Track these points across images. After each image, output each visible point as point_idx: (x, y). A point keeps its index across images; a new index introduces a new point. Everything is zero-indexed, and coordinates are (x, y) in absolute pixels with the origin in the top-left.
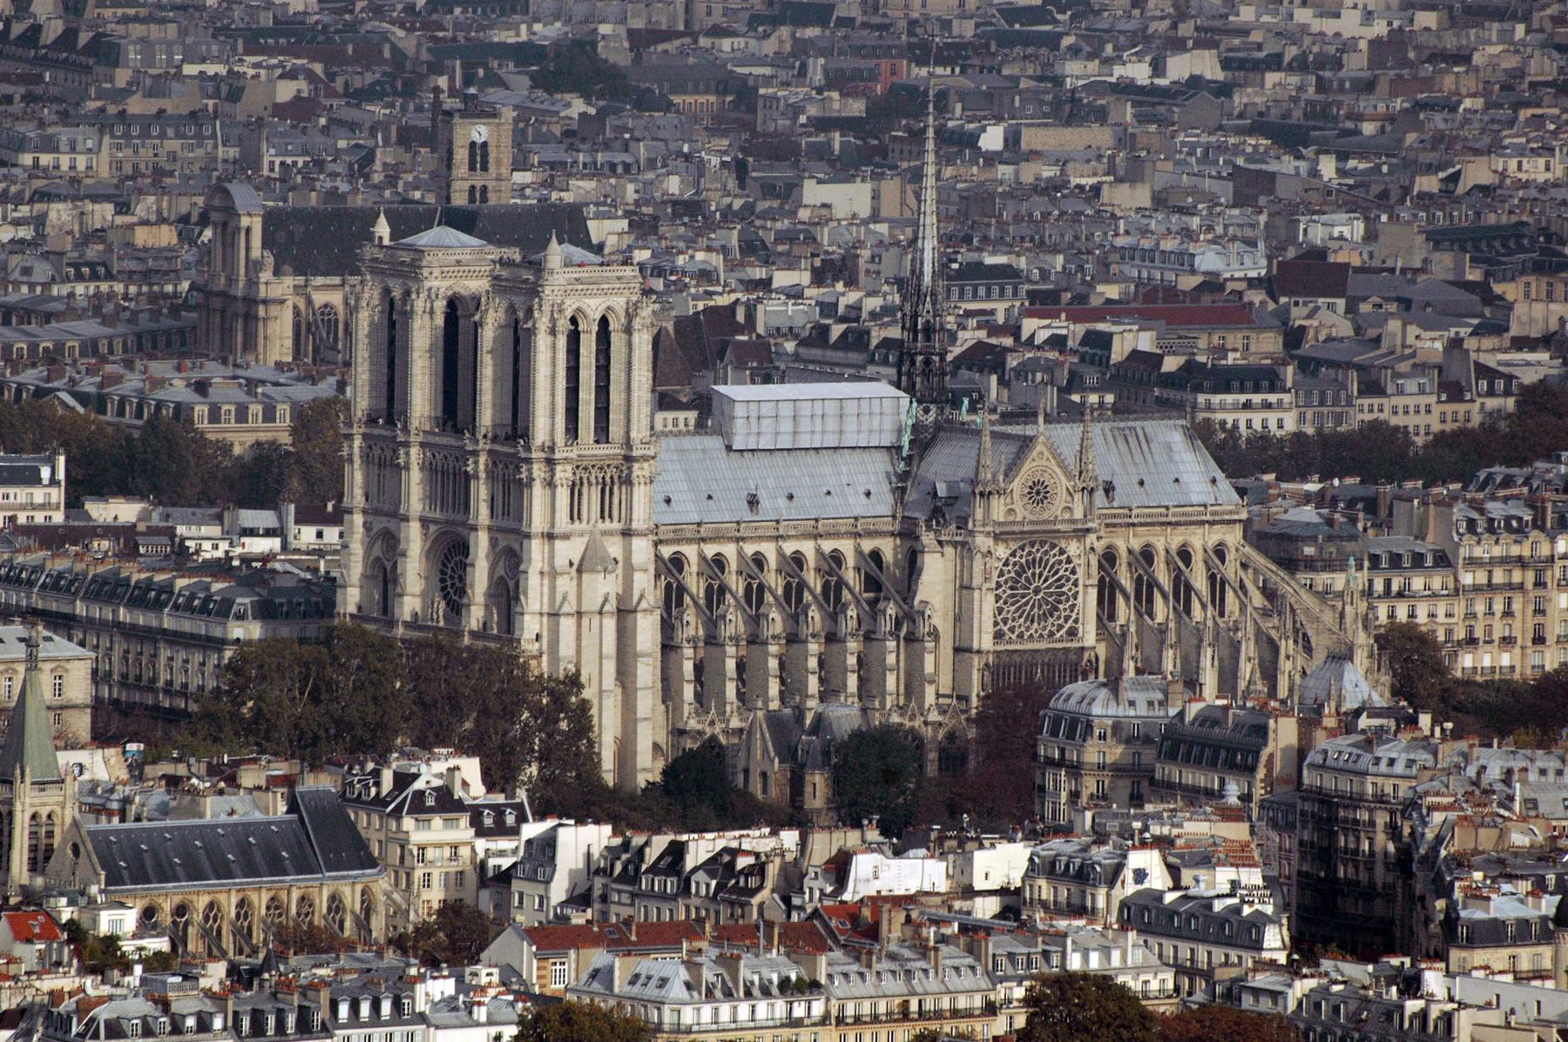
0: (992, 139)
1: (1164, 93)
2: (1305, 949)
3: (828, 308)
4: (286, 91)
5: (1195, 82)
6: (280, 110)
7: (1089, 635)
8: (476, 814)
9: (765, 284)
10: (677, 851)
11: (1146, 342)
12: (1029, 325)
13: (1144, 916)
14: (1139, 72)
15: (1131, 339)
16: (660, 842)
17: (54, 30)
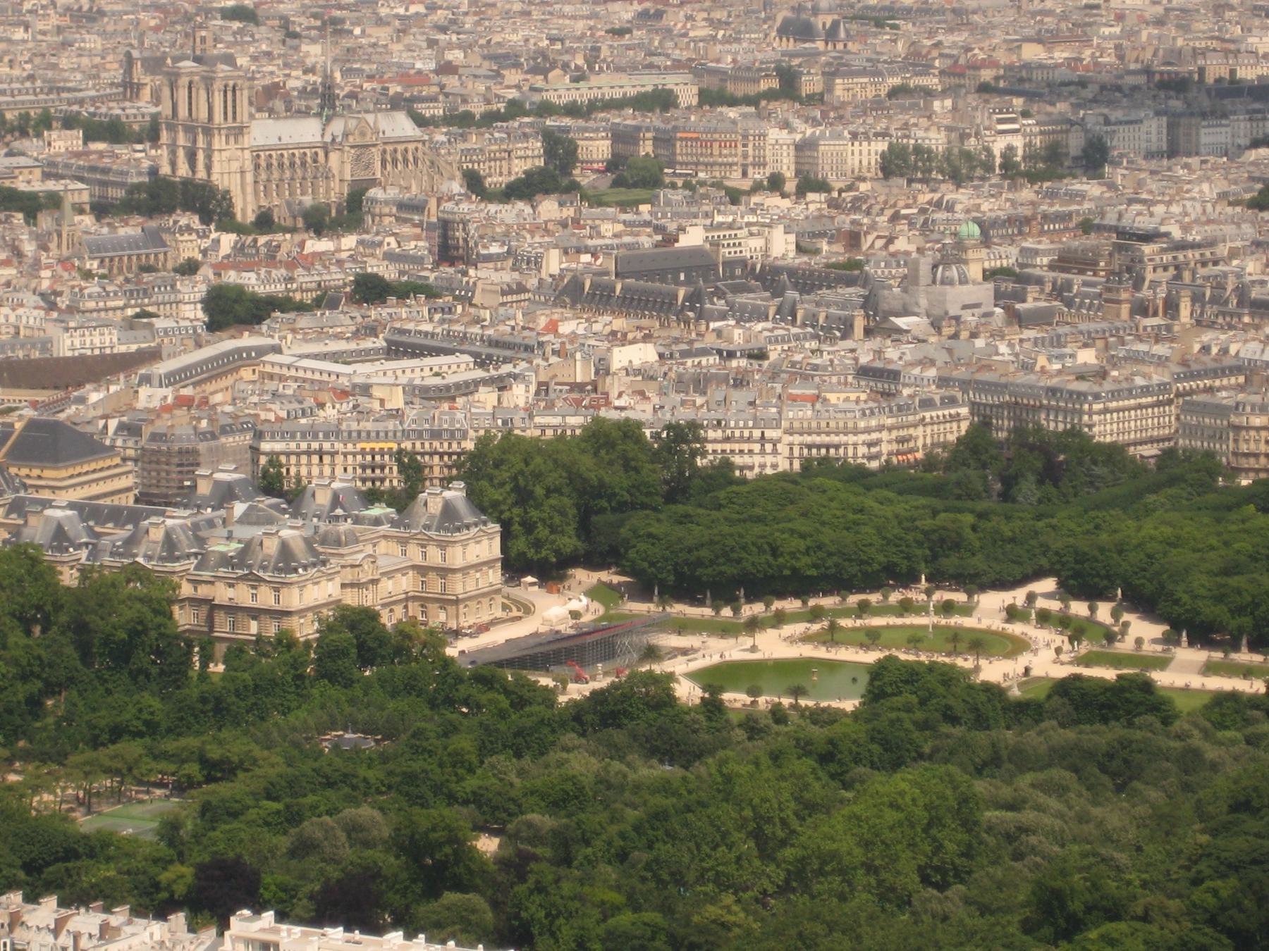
0: (357, 31)
1: (408, 17)
2: (437, 264)
3: (307, 82)
4: (153, 23)
5: (417, 13)
6: (151, 28)
7: (378, 175)
8: (197, 232)
9: (288, 76)
10: (255, 241)
11: (399, 89)
12: (365, 85)
13: (390, 257)
14: (401, 11)
15: (395, 89)
16: (250, 239)
17: (86, 8)
